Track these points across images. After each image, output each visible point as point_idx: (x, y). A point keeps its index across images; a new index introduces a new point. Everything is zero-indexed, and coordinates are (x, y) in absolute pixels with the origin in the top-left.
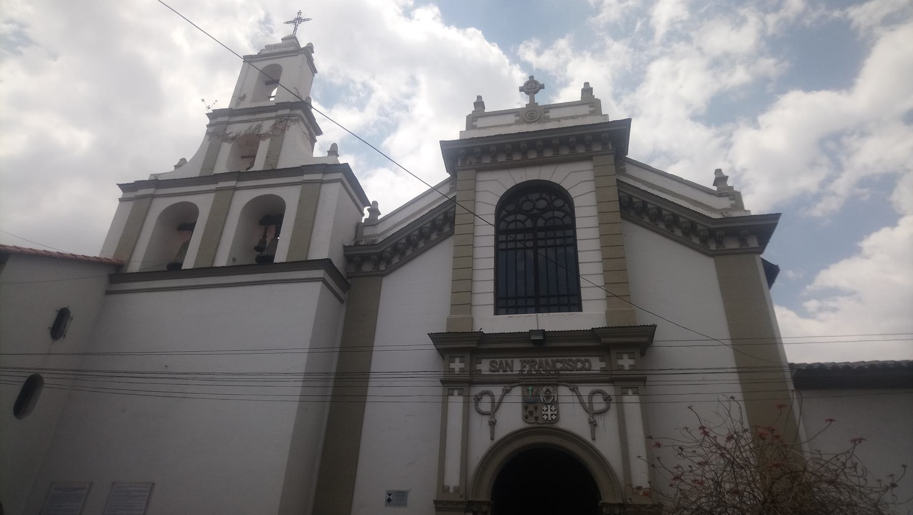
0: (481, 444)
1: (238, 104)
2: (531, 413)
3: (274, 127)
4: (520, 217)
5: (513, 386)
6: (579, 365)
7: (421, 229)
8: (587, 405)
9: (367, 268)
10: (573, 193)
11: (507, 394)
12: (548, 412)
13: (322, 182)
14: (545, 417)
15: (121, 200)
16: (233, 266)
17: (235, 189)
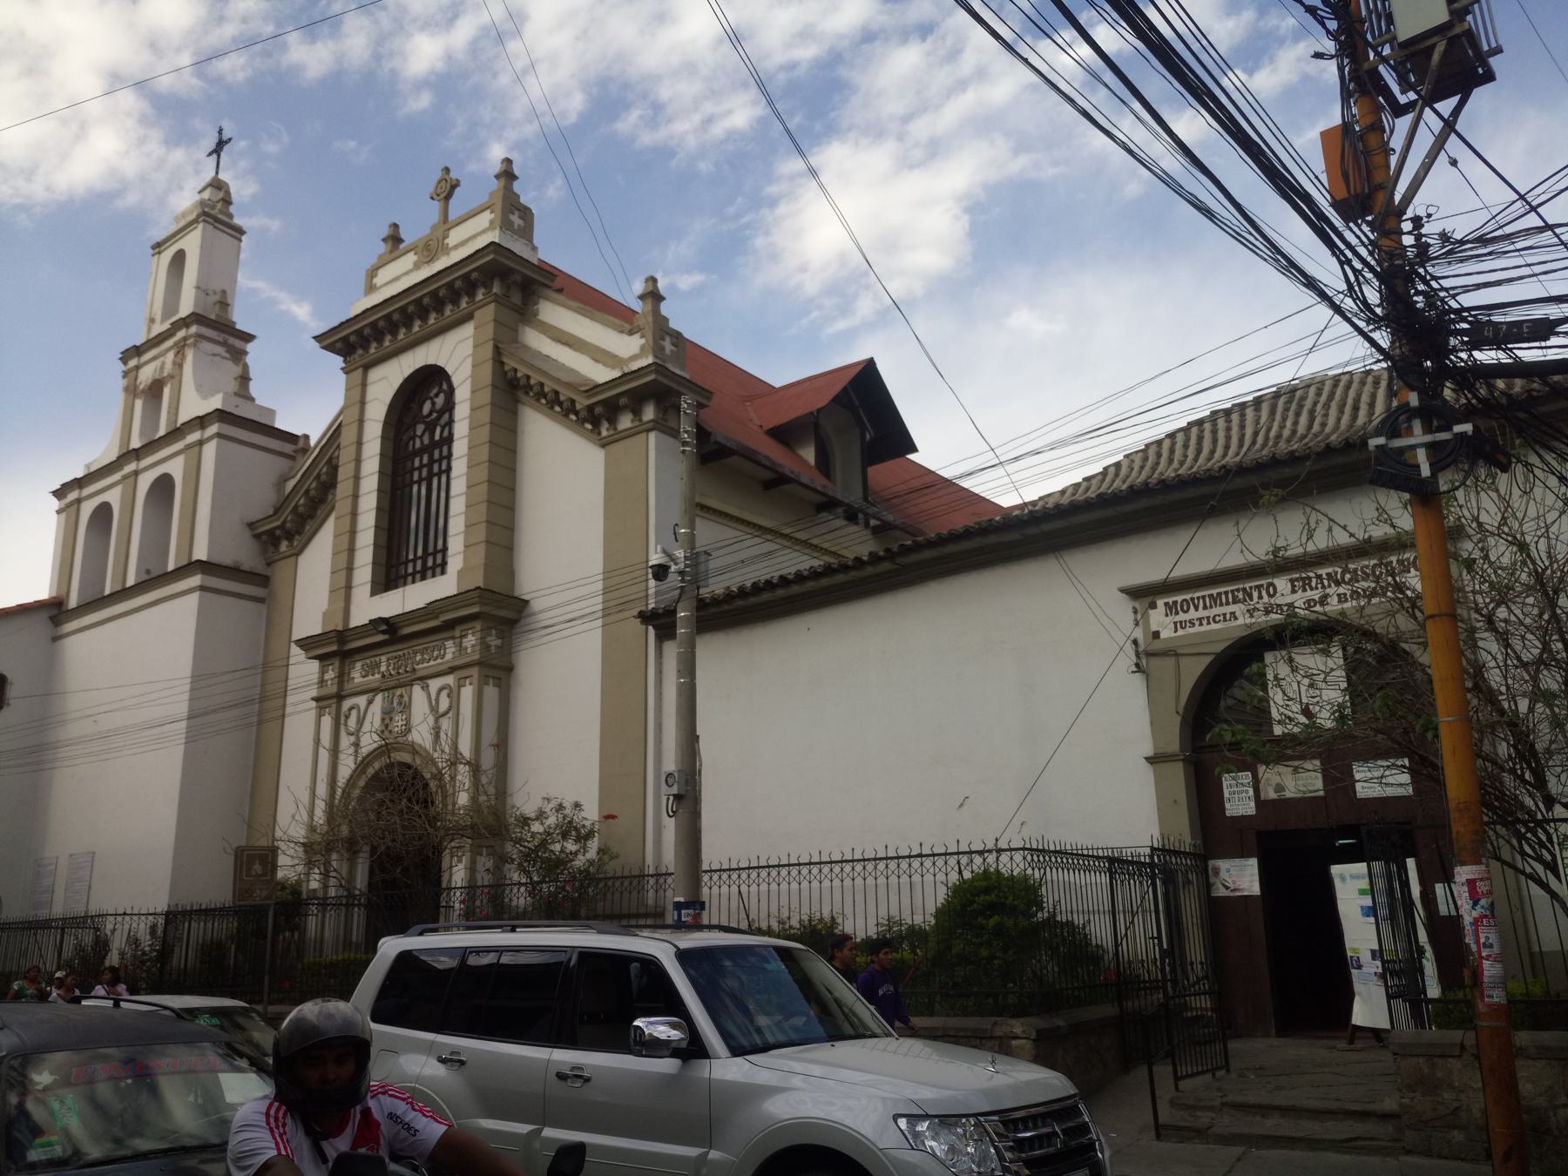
0: (345, 772)
1: (149, 330)
2: (387, 726)
3: (174, 363)
4: (420, 429)
5: (374, 696)
6: (436, 653)
7: (318, 476)
8: (434, 702)
9: (284, 545)
10: (455, 381)
11: (371, 706)
12: (398, 722)
13: (201, 443)
14: (396, 729)
15: (58, 512)
16: (146, 581)
17: (136, 473)
